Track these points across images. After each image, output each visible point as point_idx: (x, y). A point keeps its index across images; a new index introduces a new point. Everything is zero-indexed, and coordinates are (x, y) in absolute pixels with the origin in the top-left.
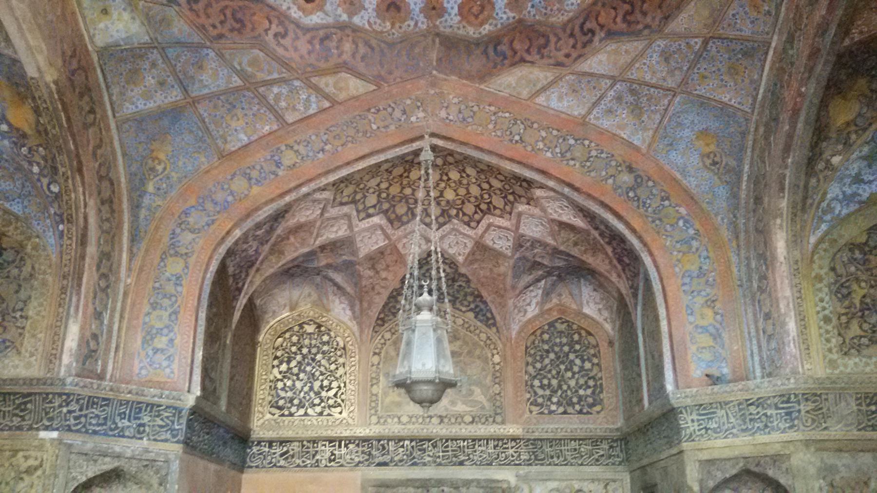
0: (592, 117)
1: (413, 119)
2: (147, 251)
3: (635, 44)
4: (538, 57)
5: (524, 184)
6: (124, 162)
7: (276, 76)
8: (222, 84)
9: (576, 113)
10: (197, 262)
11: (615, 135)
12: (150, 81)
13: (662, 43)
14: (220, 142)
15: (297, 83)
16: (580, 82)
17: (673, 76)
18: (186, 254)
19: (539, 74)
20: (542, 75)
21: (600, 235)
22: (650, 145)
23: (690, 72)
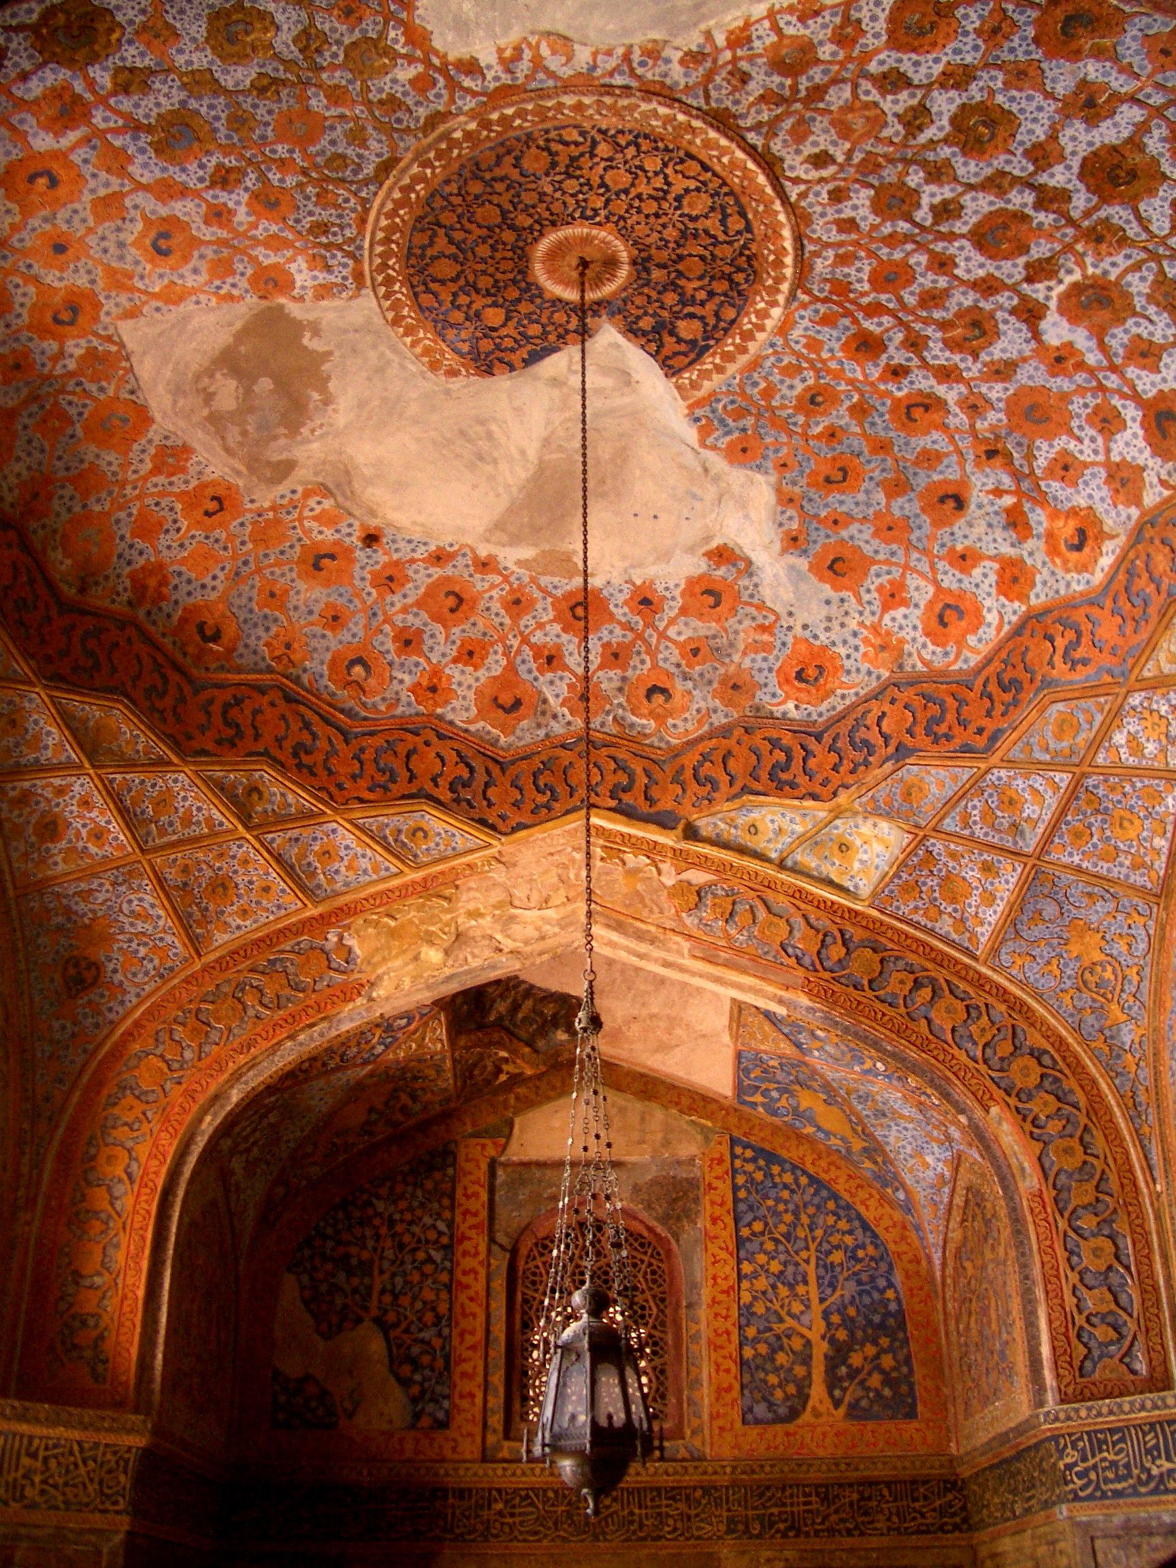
7: (1099, 718)
8: (1052, 801)
12: (972, 874)
14: (1138, 879)
15: (1136, 700)
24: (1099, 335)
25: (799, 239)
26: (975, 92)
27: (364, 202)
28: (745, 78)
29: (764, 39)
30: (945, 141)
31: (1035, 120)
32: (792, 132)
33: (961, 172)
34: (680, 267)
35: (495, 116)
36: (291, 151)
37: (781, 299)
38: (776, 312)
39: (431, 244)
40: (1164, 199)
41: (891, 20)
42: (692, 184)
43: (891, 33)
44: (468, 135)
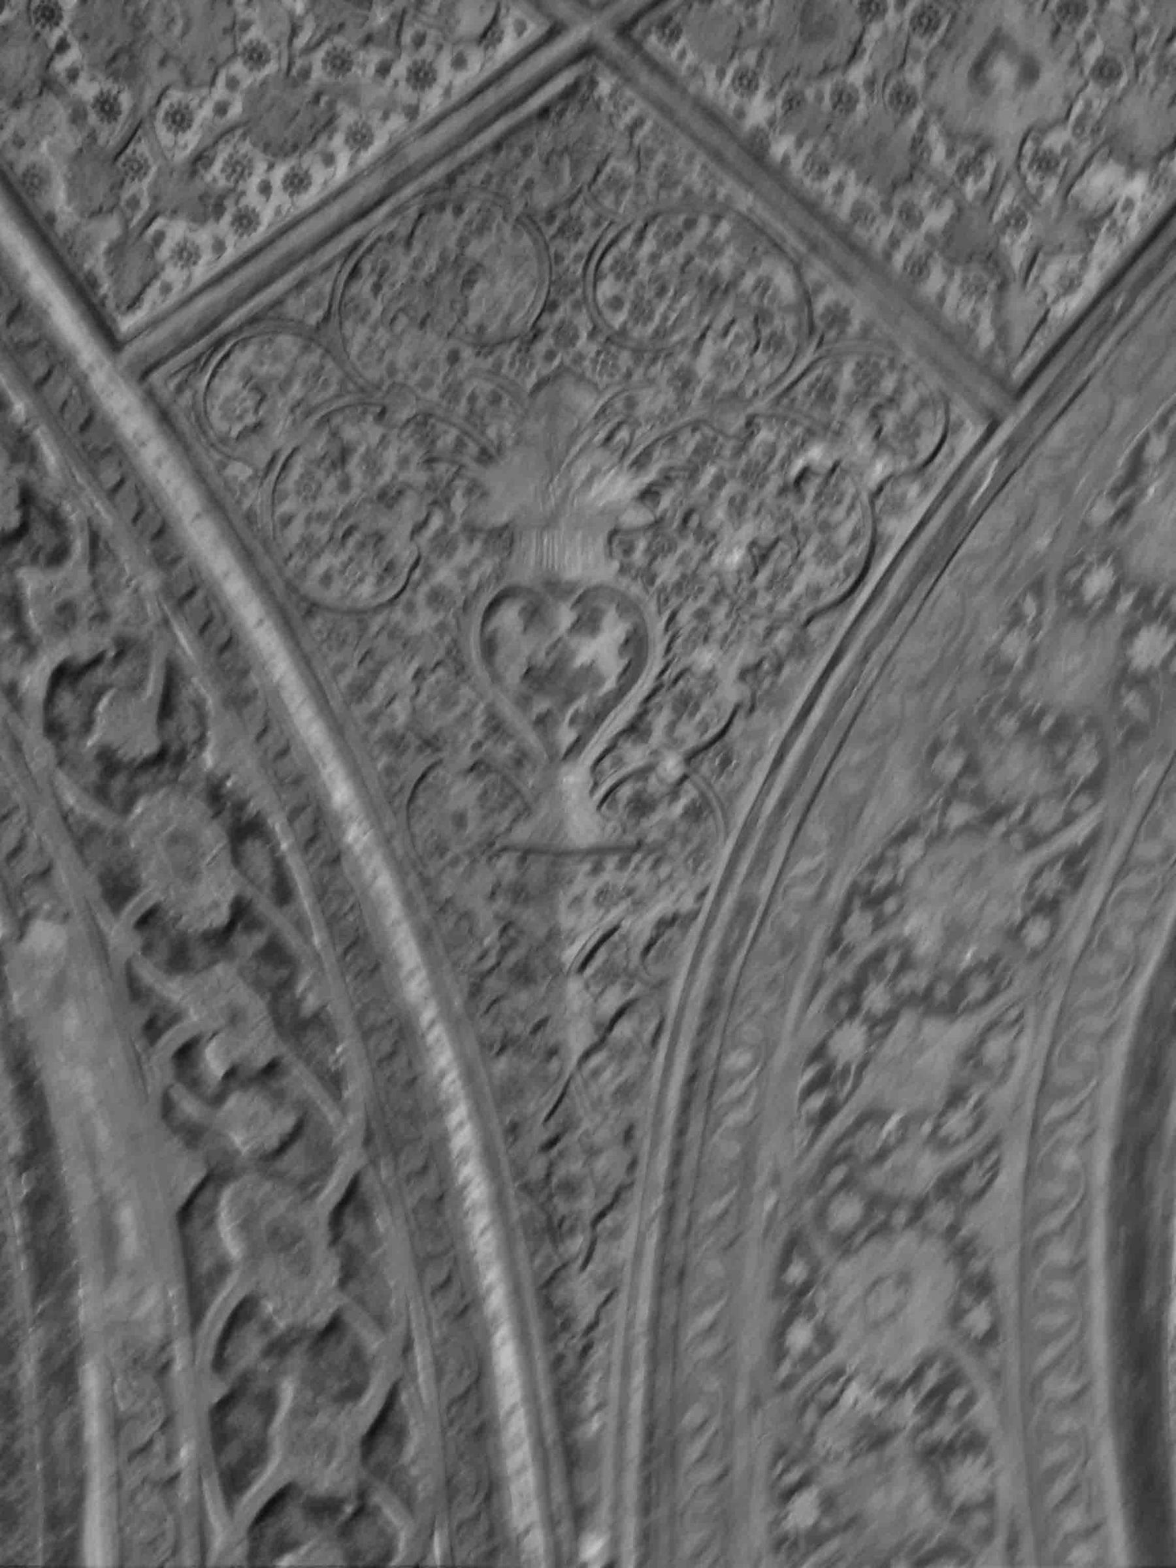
2: (673, 1276)
6: (305, 662)
10: (1032, 1216)
18: (949, 1183)
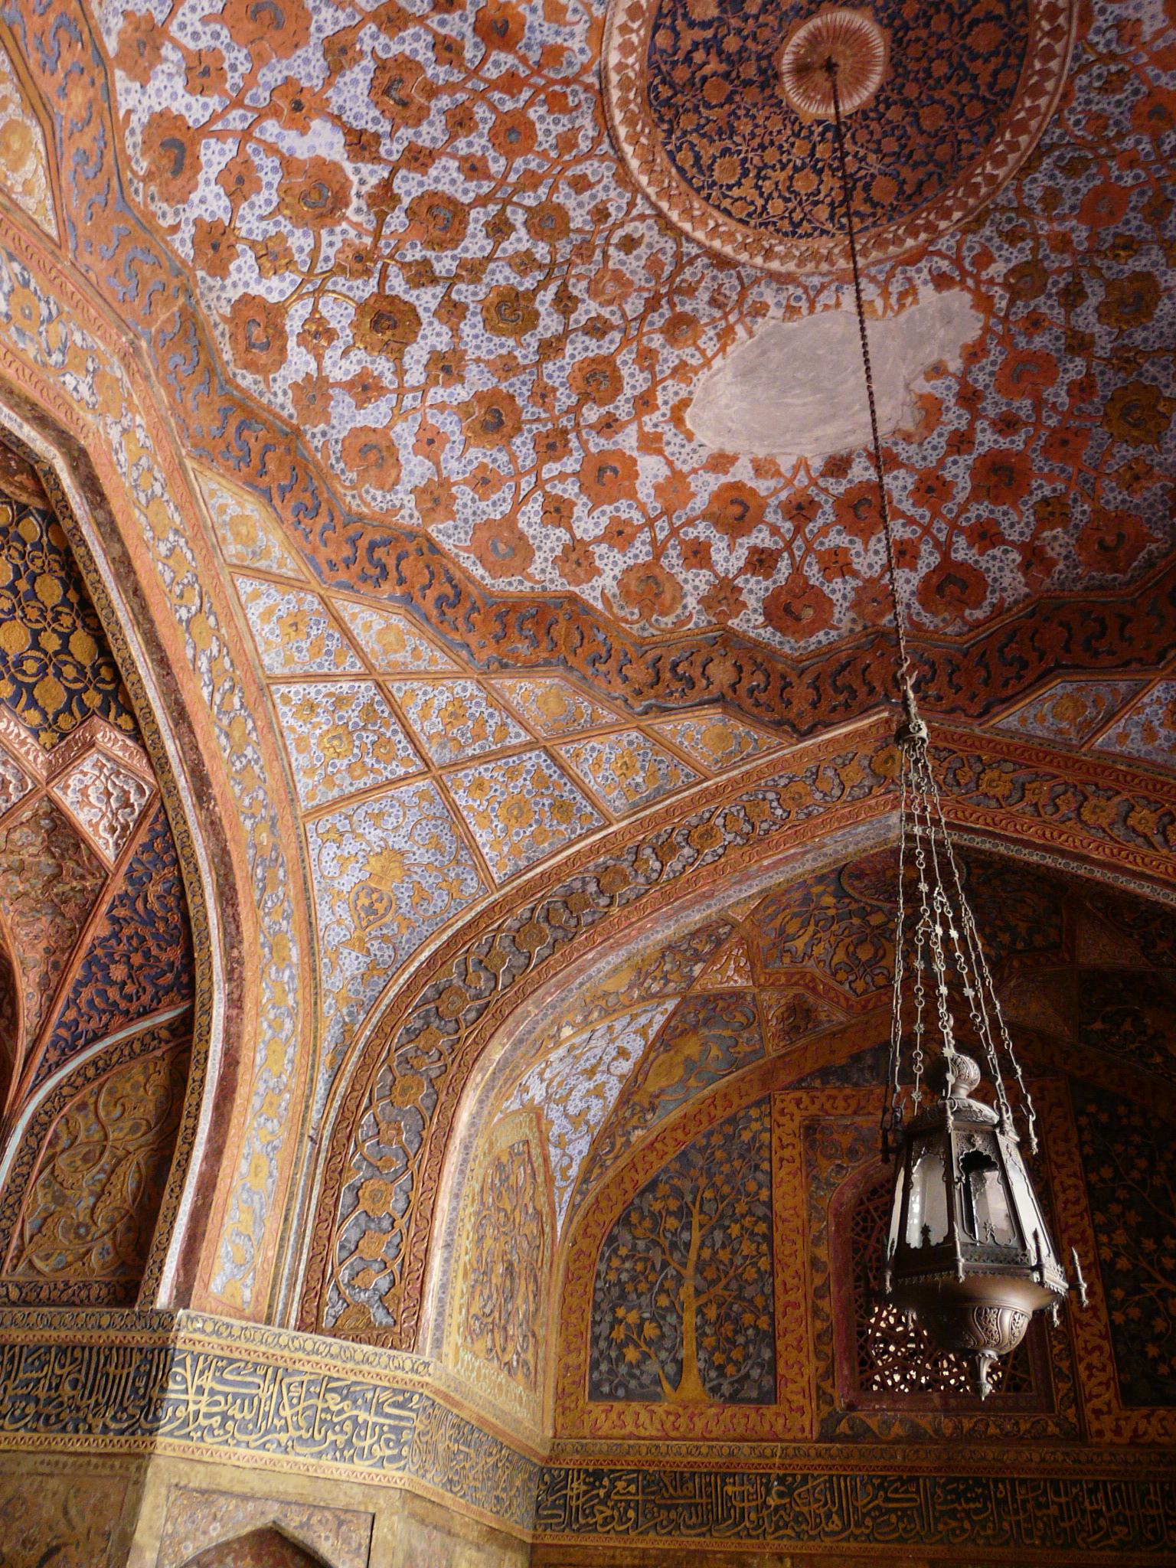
0: (284, 689)
1: (70, 380)
3: (438, 654)
4: (292, 519)
5: (93, 699)
9: (267, 661)
11: (285, 748)
13: (472, 687)
16: (318, 623)
17: (443, 746)
19: (276, 546)
20: (277, 552)
21: (122, 898)
22: (318, 809)
23: (475, 763)
24: (288, 164)
25: (621, 160)
26: (532, 340)
27: (1058, 122)
28: (713, 302)
29: (708, 342)
30: (535, 292)
31: (476, 337)
32: (662, 265)
33: (507, 271)
34: (730, 88)
35: (923, 236)
36: (1119, 178)
37: (614, 78)
38: (614, 58)
39: (995, 74)
40: (343, 329)
41: (620, 378)
42: (736, 192)
43: (616, 369)
44: (946, 214)
